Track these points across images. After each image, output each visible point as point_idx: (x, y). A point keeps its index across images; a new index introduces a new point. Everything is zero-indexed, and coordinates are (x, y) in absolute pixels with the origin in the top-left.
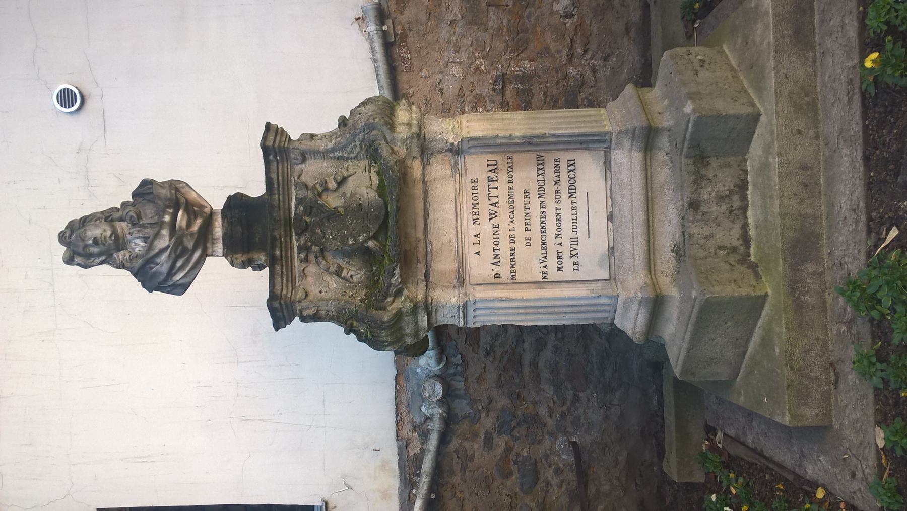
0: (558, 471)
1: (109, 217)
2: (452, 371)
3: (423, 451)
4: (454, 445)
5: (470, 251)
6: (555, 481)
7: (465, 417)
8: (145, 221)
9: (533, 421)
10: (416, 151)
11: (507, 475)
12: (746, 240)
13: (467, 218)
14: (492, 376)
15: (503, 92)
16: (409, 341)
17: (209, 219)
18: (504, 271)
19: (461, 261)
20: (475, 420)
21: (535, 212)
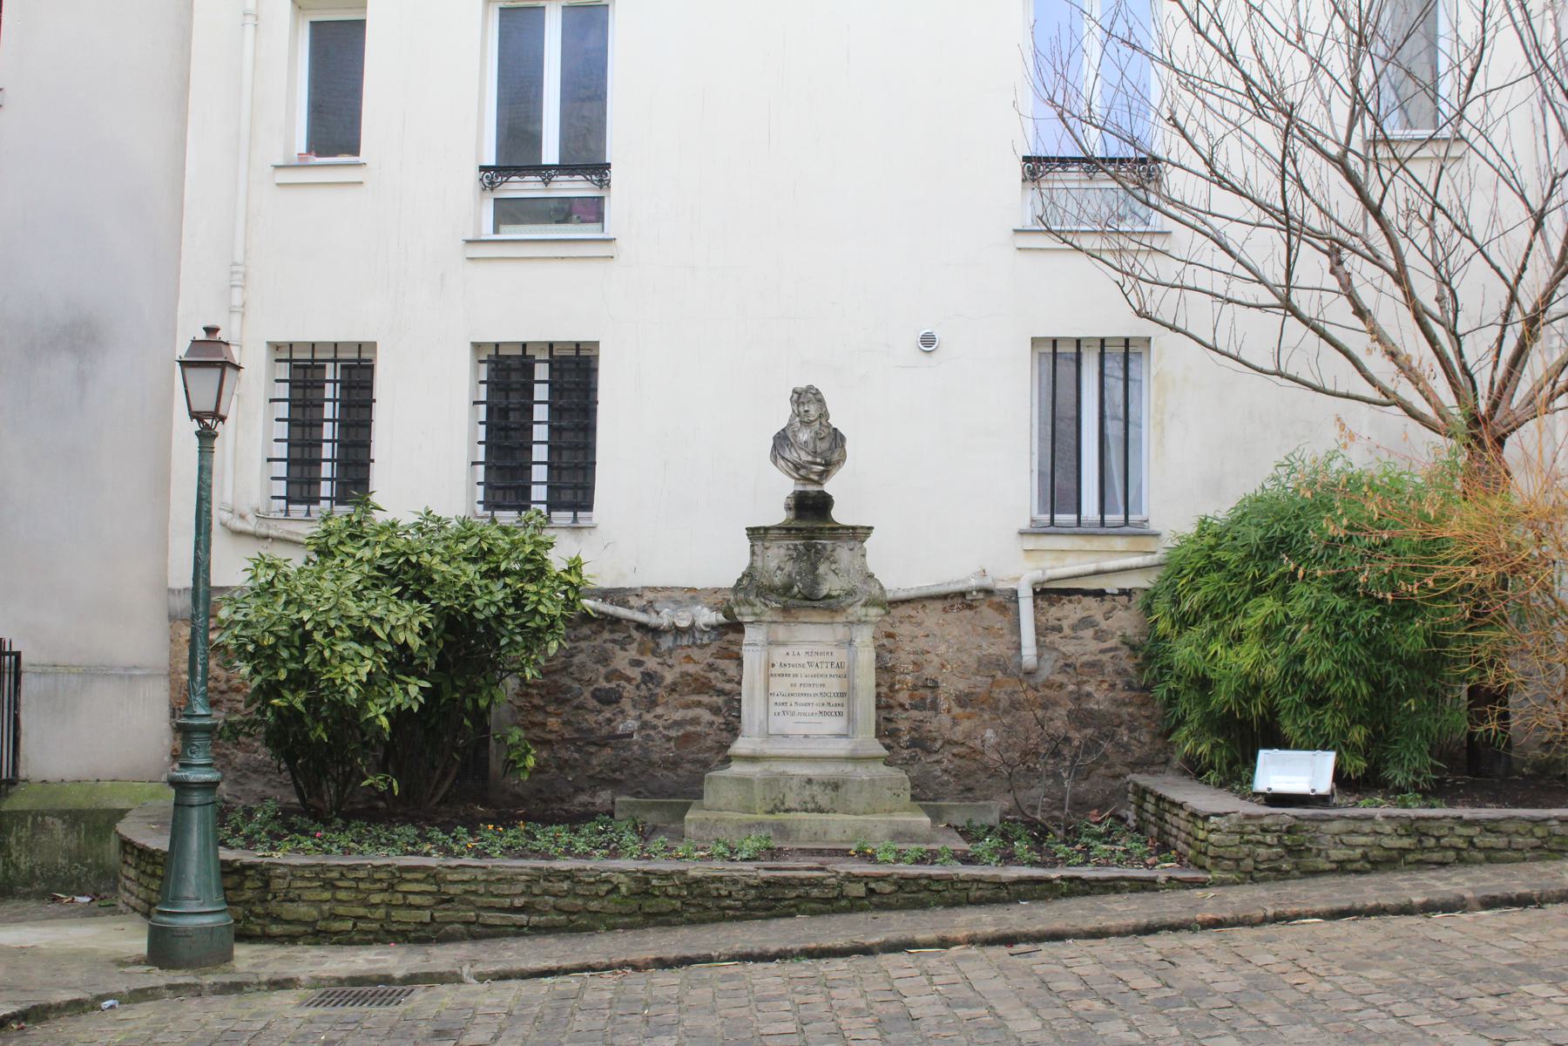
0: (609, 721)
1: (824, 415)
2: (697, 635)
3: (631, 608)
4: (636, 634)
5: (789, 649)
6: (600, 718)
7: (658, 644)
8: (818, 443)
9: (652, 702)
10: (851, 619)
11: (608, 679)
12: (787, 811)
13: (809, 648)
14: (691, 668)
15: (925, 686)
16: (736, 610)
17: (819, 483)
18: (777, 670)
19: (784, 644)
20: (654, 653)
21: (811, 691)
